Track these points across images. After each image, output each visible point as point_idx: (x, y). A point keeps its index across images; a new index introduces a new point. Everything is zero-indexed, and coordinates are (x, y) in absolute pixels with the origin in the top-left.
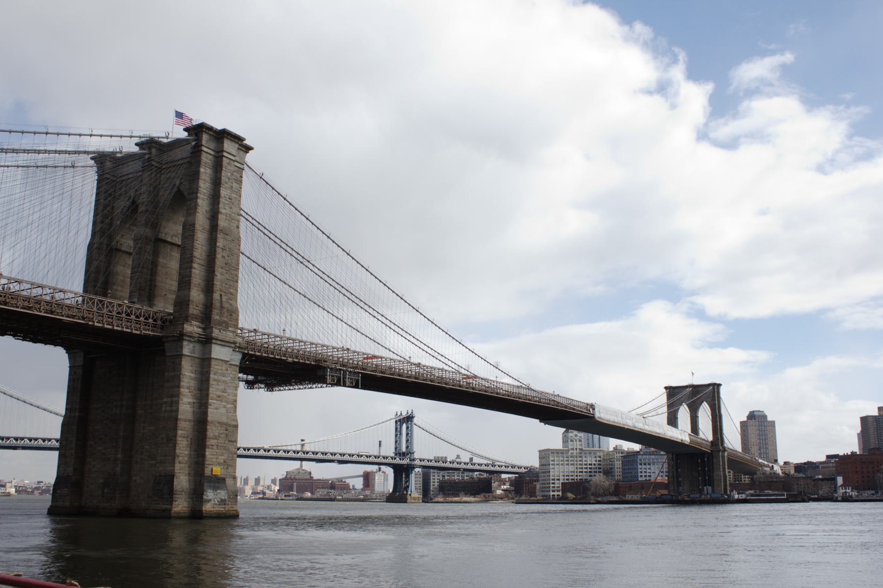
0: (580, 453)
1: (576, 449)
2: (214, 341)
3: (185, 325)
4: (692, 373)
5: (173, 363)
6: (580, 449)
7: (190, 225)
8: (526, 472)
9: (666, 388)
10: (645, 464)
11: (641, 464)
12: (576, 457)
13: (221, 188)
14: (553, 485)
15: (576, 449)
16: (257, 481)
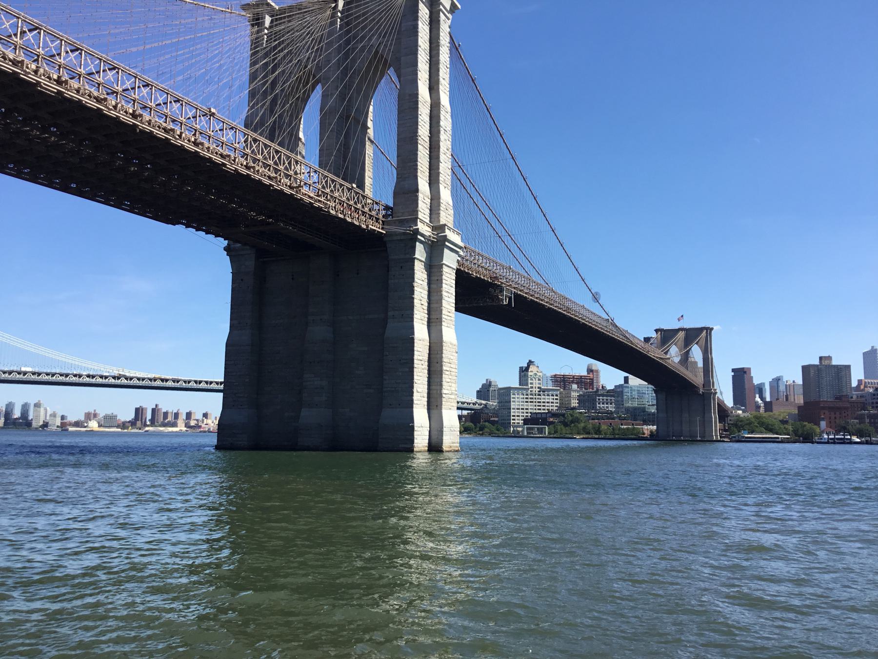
0: (539, 391)
1: (535, 387)
2: (447, 243)
3: (419, 220)
4: (682, 316)
5: (402, 267)
6: (539, 388)
7: (410, 95)
8: (482, 409)
9: (657, 331)
10: (603, 404)
11: (599, 404)
12: (535, 395)
13: (441, 52)
14: (514, 421)
15: (535, 387)
16: (189, 415)
